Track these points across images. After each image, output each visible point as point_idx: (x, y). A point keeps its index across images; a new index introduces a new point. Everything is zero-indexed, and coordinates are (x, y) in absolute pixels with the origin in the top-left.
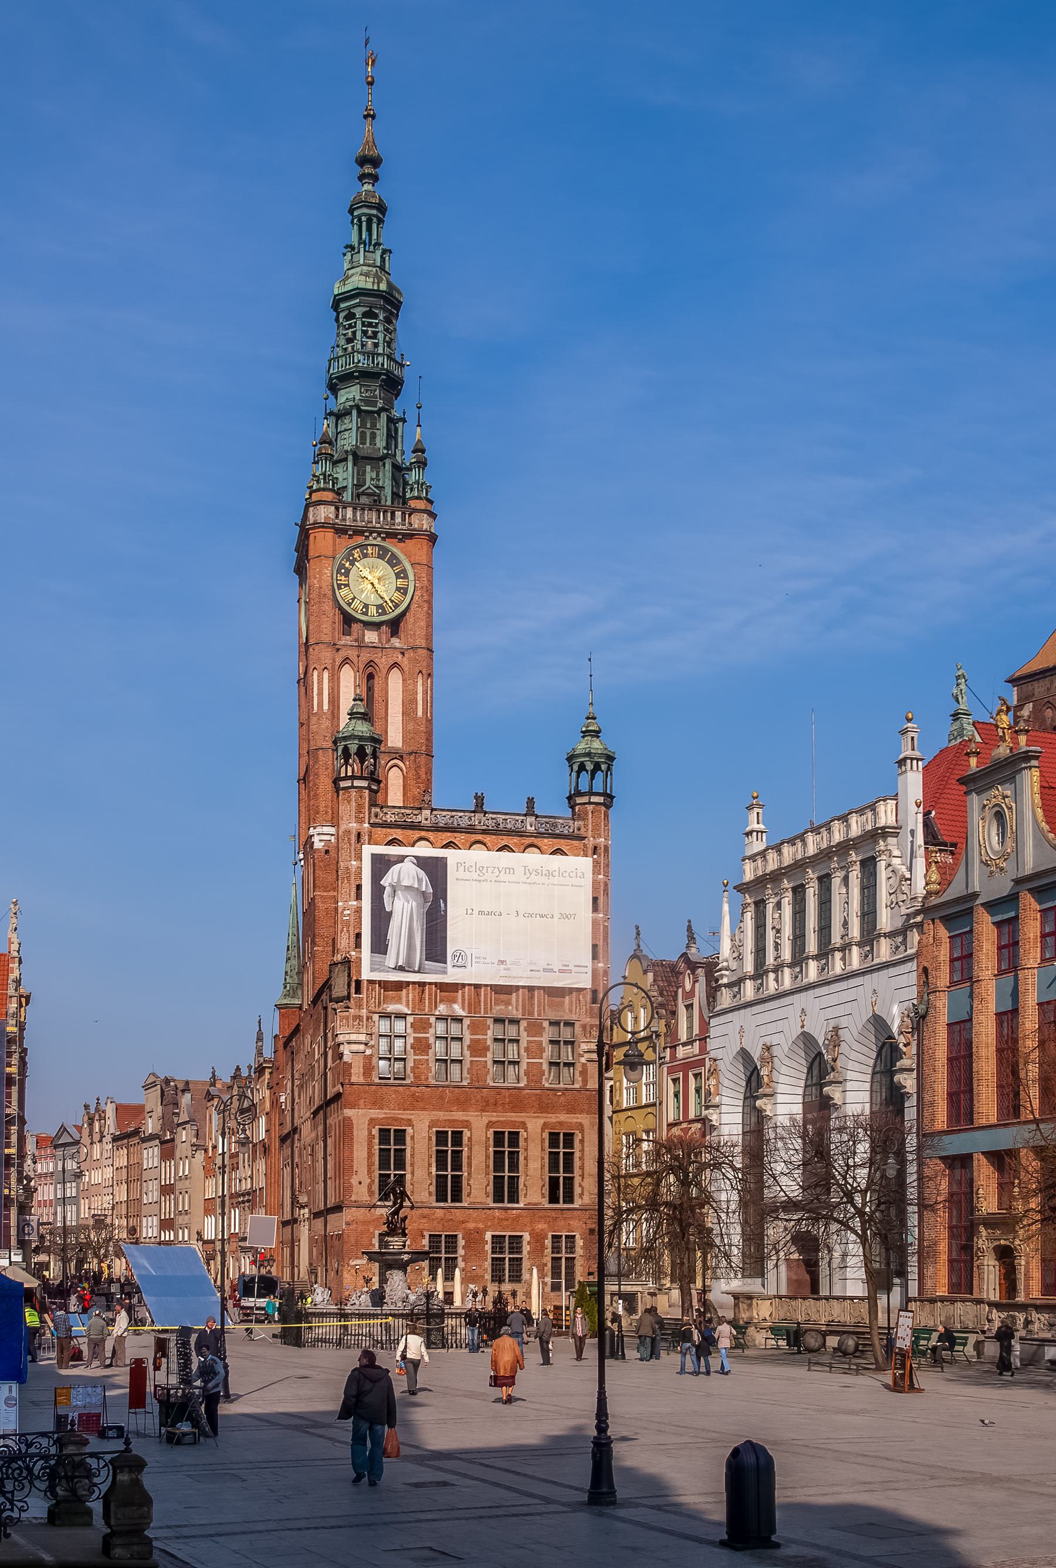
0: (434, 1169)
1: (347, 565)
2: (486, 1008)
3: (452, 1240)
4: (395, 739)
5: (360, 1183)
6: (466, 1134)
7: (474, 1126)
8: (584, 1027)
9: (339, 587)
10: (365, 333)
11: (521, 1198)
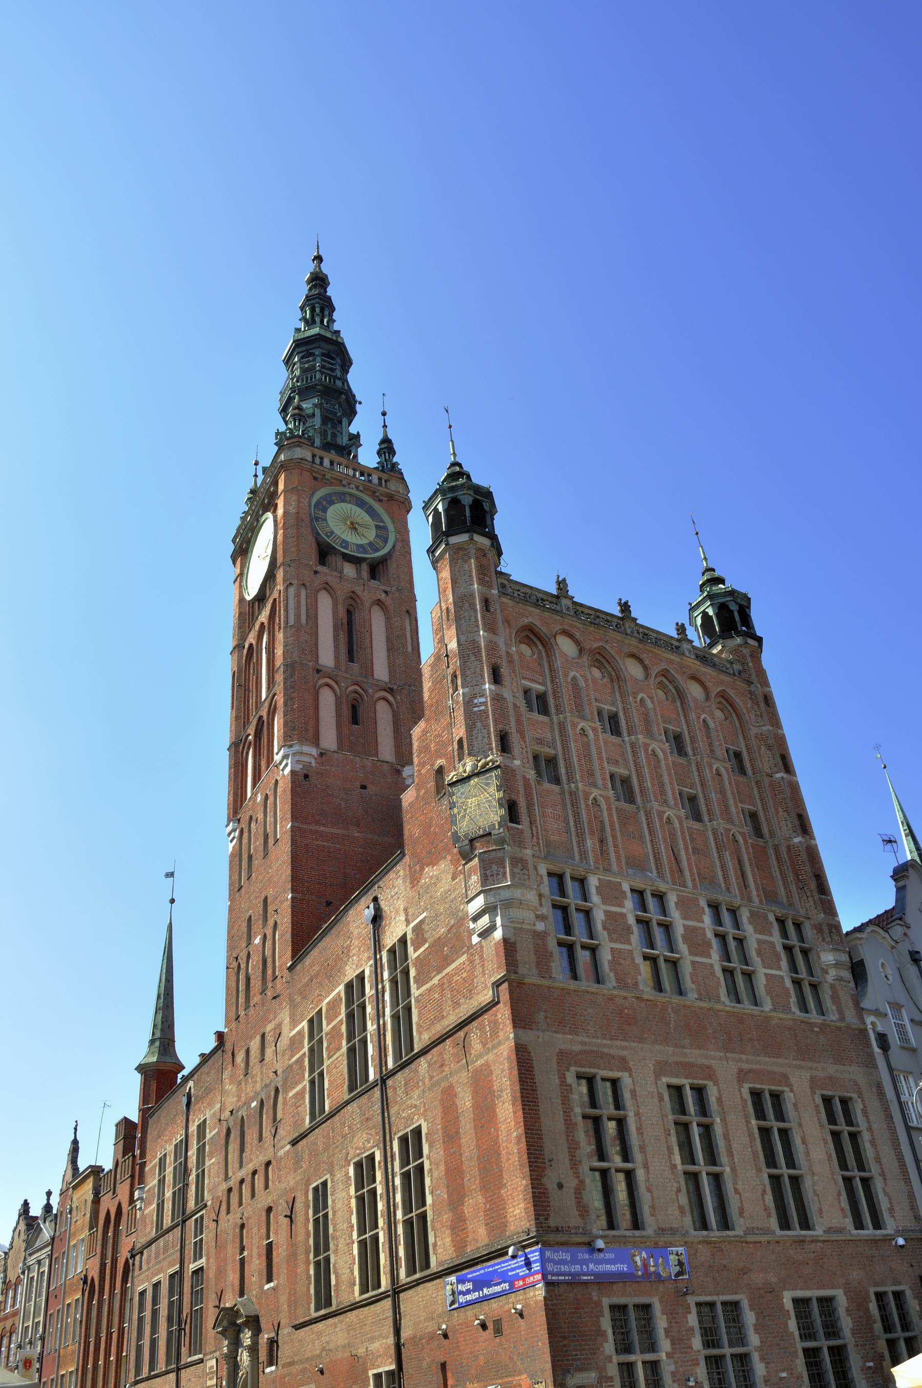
0: (677, 1159)
1: (324, 503)
2: (693, 880)
3: (733, 1307)
4: (381, 671)
5: (560, 1186)
6: (712, 1094)
8: (818, 928)
9: (317, 519)
10: (322, 367)
11: (815, 1218)
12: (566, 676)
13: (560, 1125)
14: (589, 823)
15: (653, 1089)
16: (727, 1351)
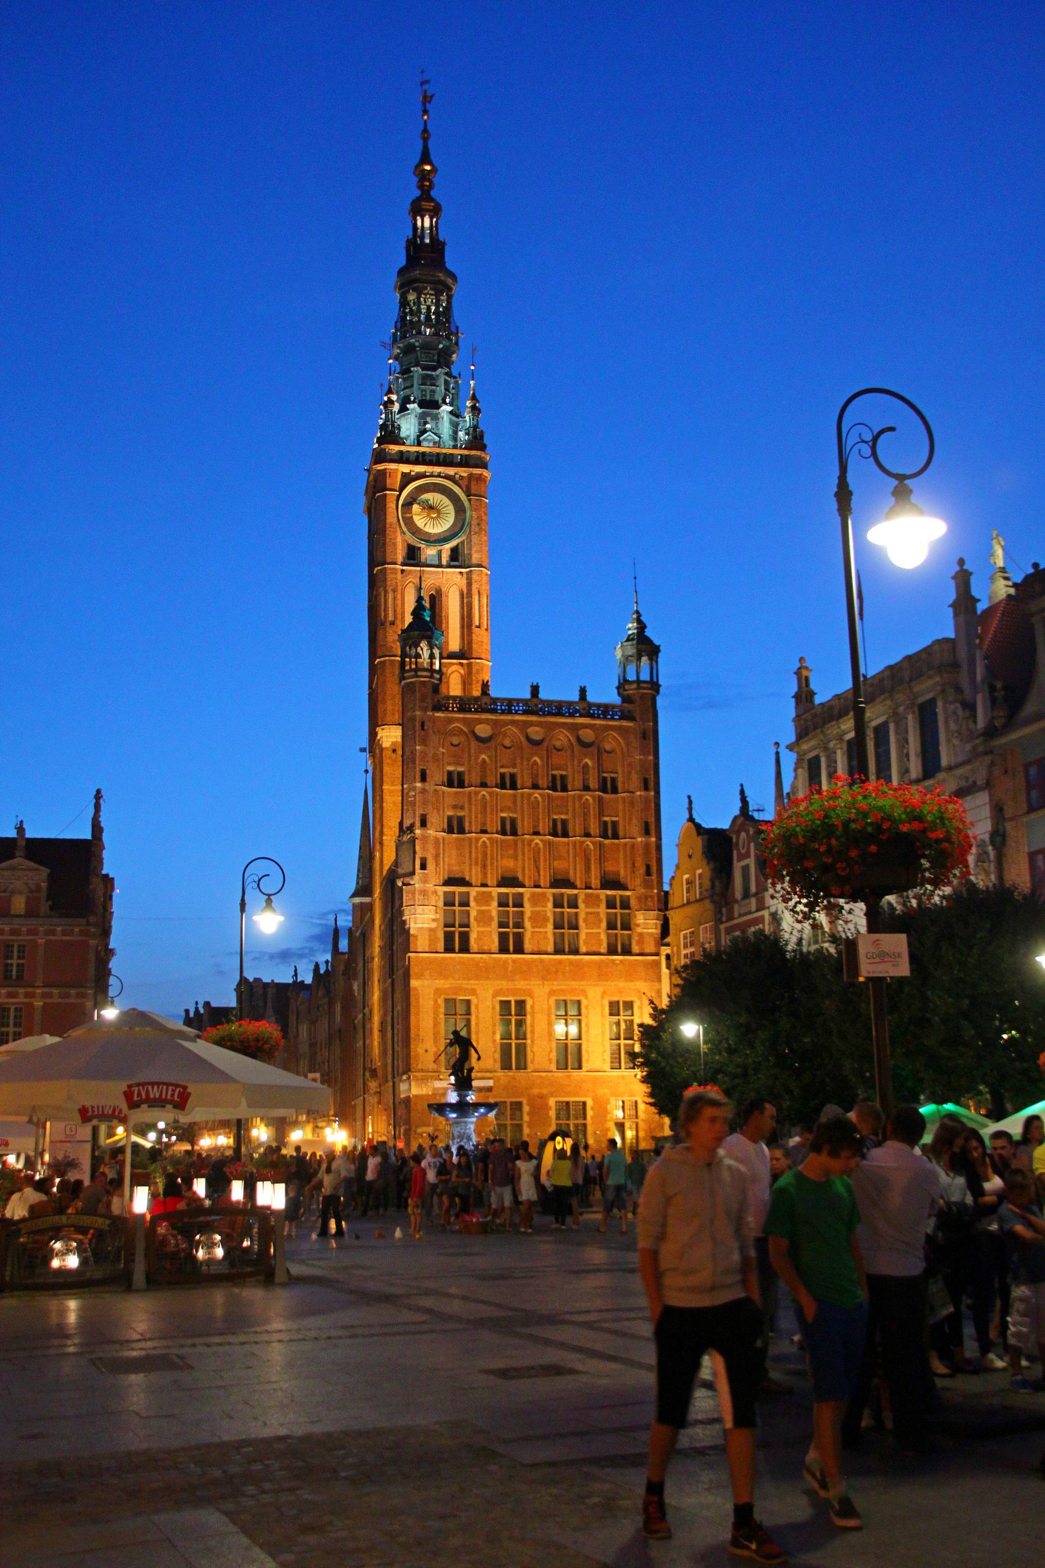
0: (498, 1037)
5: (426, 1051)
7: (536, 994)
12: (477, 758)
13: (431, 1024)
14: (477, 859)
15: (489, 1003)
16: (509, 1122)
